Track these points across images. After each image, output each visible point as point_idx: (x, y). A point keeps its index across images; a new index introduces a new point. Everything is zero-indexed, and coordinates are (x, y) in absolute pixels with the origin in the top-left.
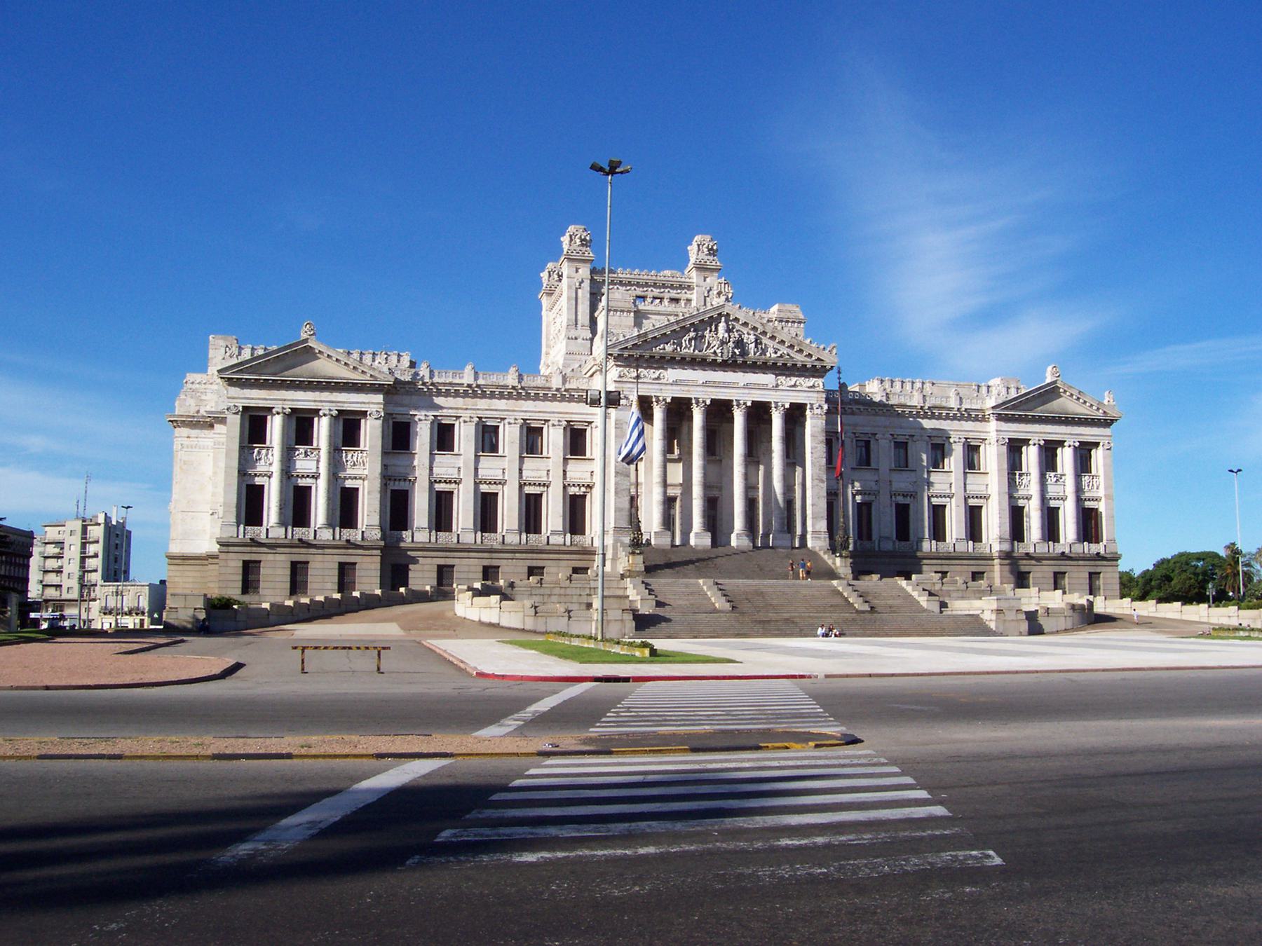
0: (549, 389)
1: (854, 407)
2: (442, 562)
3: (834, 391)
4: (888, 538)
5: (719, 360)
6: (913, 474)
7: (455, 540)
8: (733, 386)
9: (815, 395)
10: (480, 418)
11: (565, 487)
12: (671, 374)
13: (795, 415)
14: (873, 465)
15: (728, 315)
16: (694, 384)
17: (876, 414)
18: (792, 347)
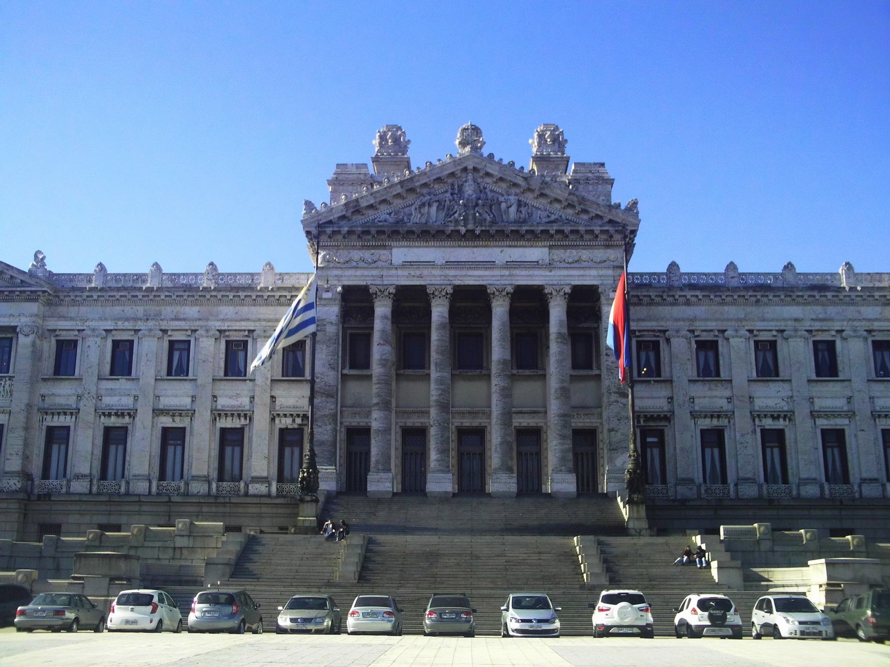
0: (250, 288)
1: (689, 294)
2: (104, 520)
3: (659, 275)
4: (752, 480)
5: (463, 230)
6: (786, 386)
7: (123, 490)
8: (489, 265)
9: (610, 272)
10: (165, 331)
11: (273, 419)
12: (400, 253)
13: (585, 303)
14: (724, 375)
15: (475, 169)
16: (431, 264)
17: (723, 303)
18: (571, 206)
